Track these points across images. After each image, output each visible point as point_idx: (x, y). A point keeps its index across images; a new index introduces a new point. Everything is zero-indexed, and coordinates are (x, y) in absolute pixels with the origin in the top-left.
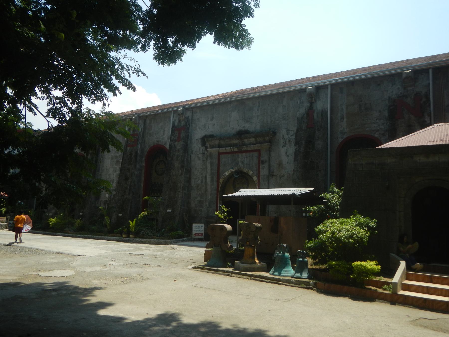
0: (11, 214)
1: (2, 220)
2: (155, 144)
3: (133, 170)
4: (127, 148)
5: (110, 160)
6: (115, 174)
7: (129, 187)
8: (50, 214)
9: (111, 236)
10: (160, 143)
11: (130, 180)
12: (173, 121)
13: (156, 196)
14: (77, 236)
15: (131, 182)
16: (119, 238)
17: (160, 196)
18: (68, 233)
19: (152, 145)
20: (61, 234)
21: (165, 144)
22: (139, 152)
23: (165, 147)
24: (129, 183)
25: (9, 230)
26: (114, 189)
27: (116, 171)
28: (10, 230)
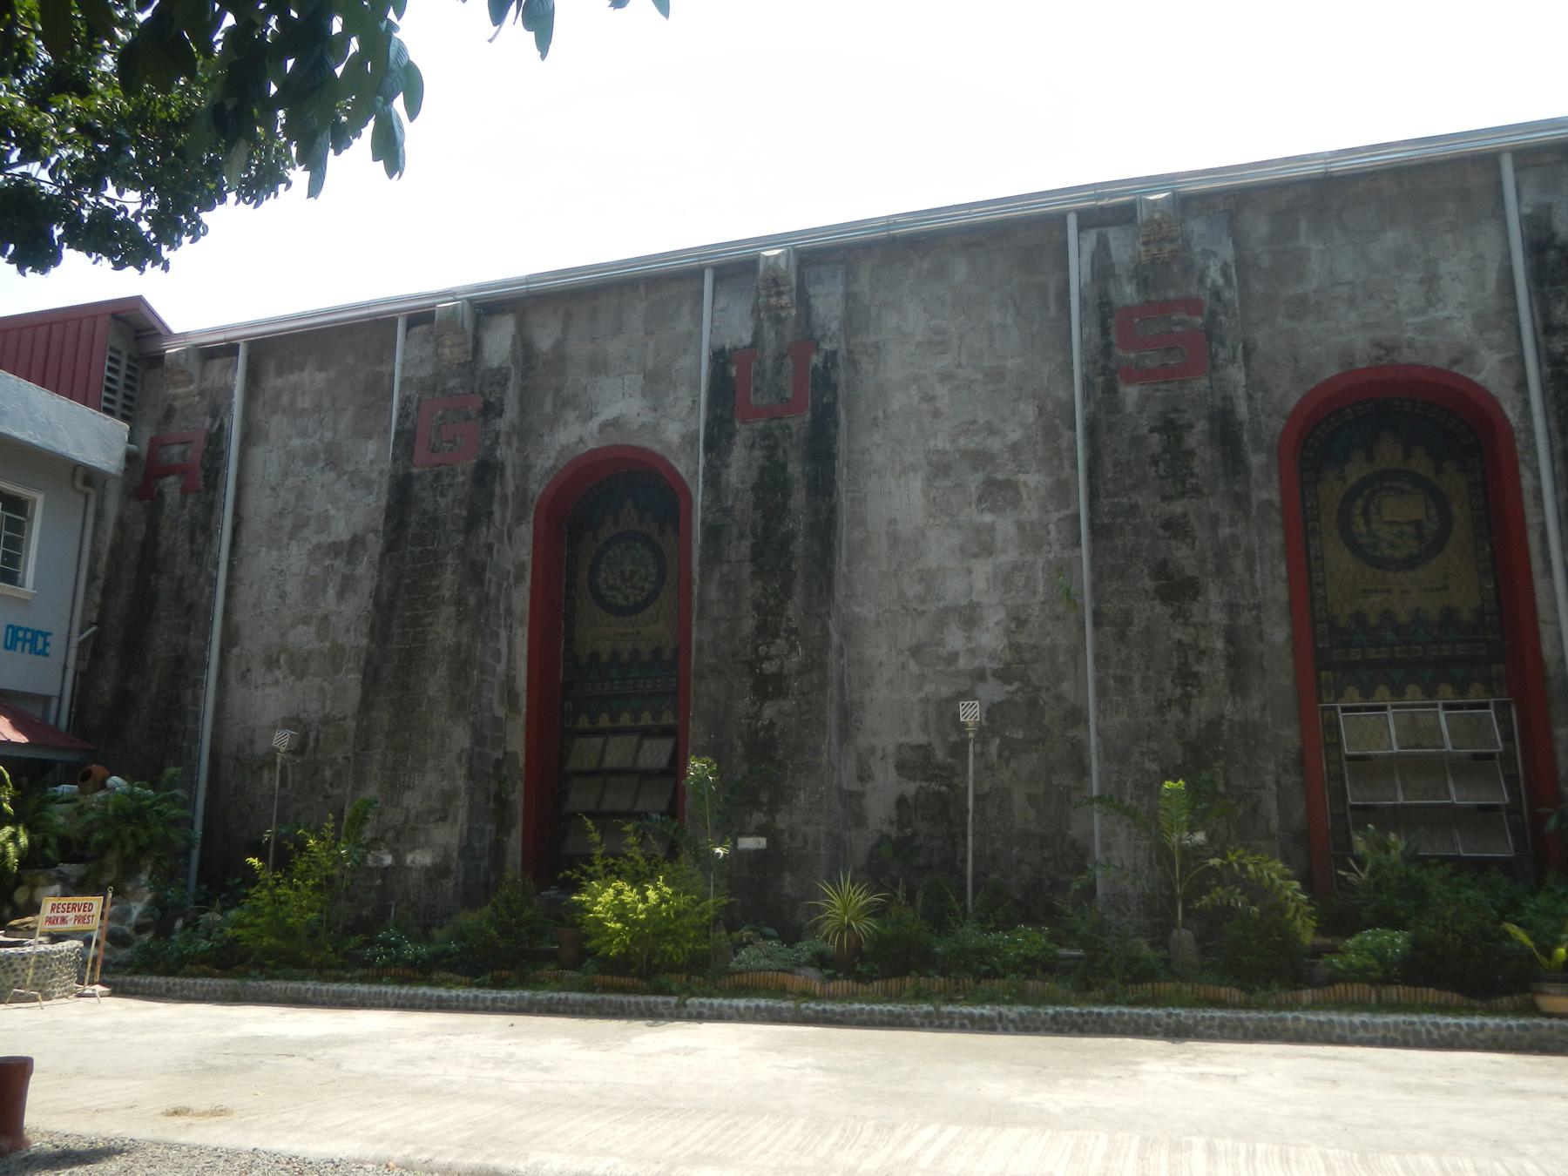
0: (66, 868)
1: (78, 919)
2: (1359, 366)
3: (1224, 531)
4: (1111, 388)
5: (916, 483)
6: (983, 570)
7: (1219, 645)
8: (409, 858)
9: (1315, 1006)
10: (1406, 357)
11: (1214, 595)
12: (1527, 210)
13: (1394, 707)
14: (950, 1015)
15: (1232, 608)
16: (1513, 1023)
17: (1435, 706)
18: (782, 992)
19: (1331, 371)
20: (741, 1003)
21: (1455, 362)
22: (1242, 410)
23: (1470, 382)
24: (1217, 616)
25: (113, 994)
26: (994, 665)
27: (988, 550)
28: (118, 991)
